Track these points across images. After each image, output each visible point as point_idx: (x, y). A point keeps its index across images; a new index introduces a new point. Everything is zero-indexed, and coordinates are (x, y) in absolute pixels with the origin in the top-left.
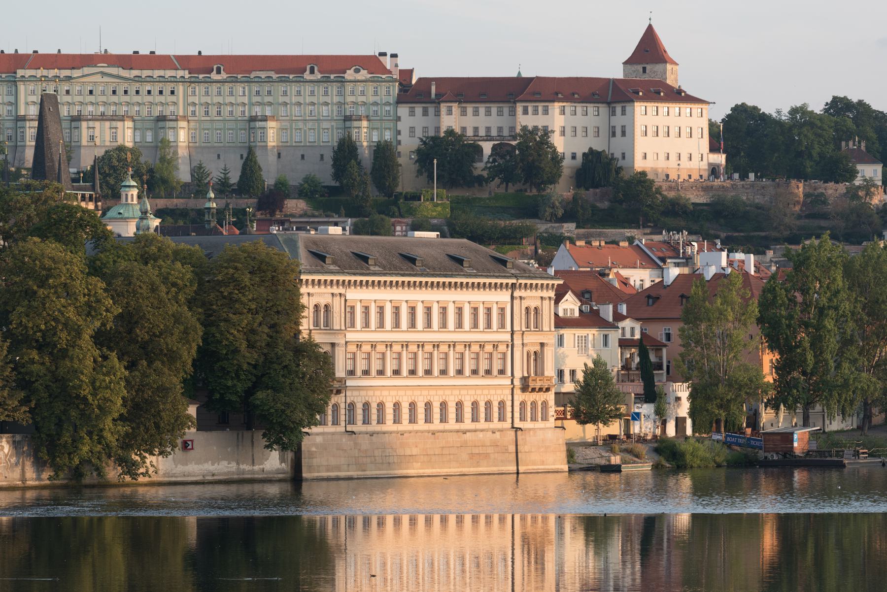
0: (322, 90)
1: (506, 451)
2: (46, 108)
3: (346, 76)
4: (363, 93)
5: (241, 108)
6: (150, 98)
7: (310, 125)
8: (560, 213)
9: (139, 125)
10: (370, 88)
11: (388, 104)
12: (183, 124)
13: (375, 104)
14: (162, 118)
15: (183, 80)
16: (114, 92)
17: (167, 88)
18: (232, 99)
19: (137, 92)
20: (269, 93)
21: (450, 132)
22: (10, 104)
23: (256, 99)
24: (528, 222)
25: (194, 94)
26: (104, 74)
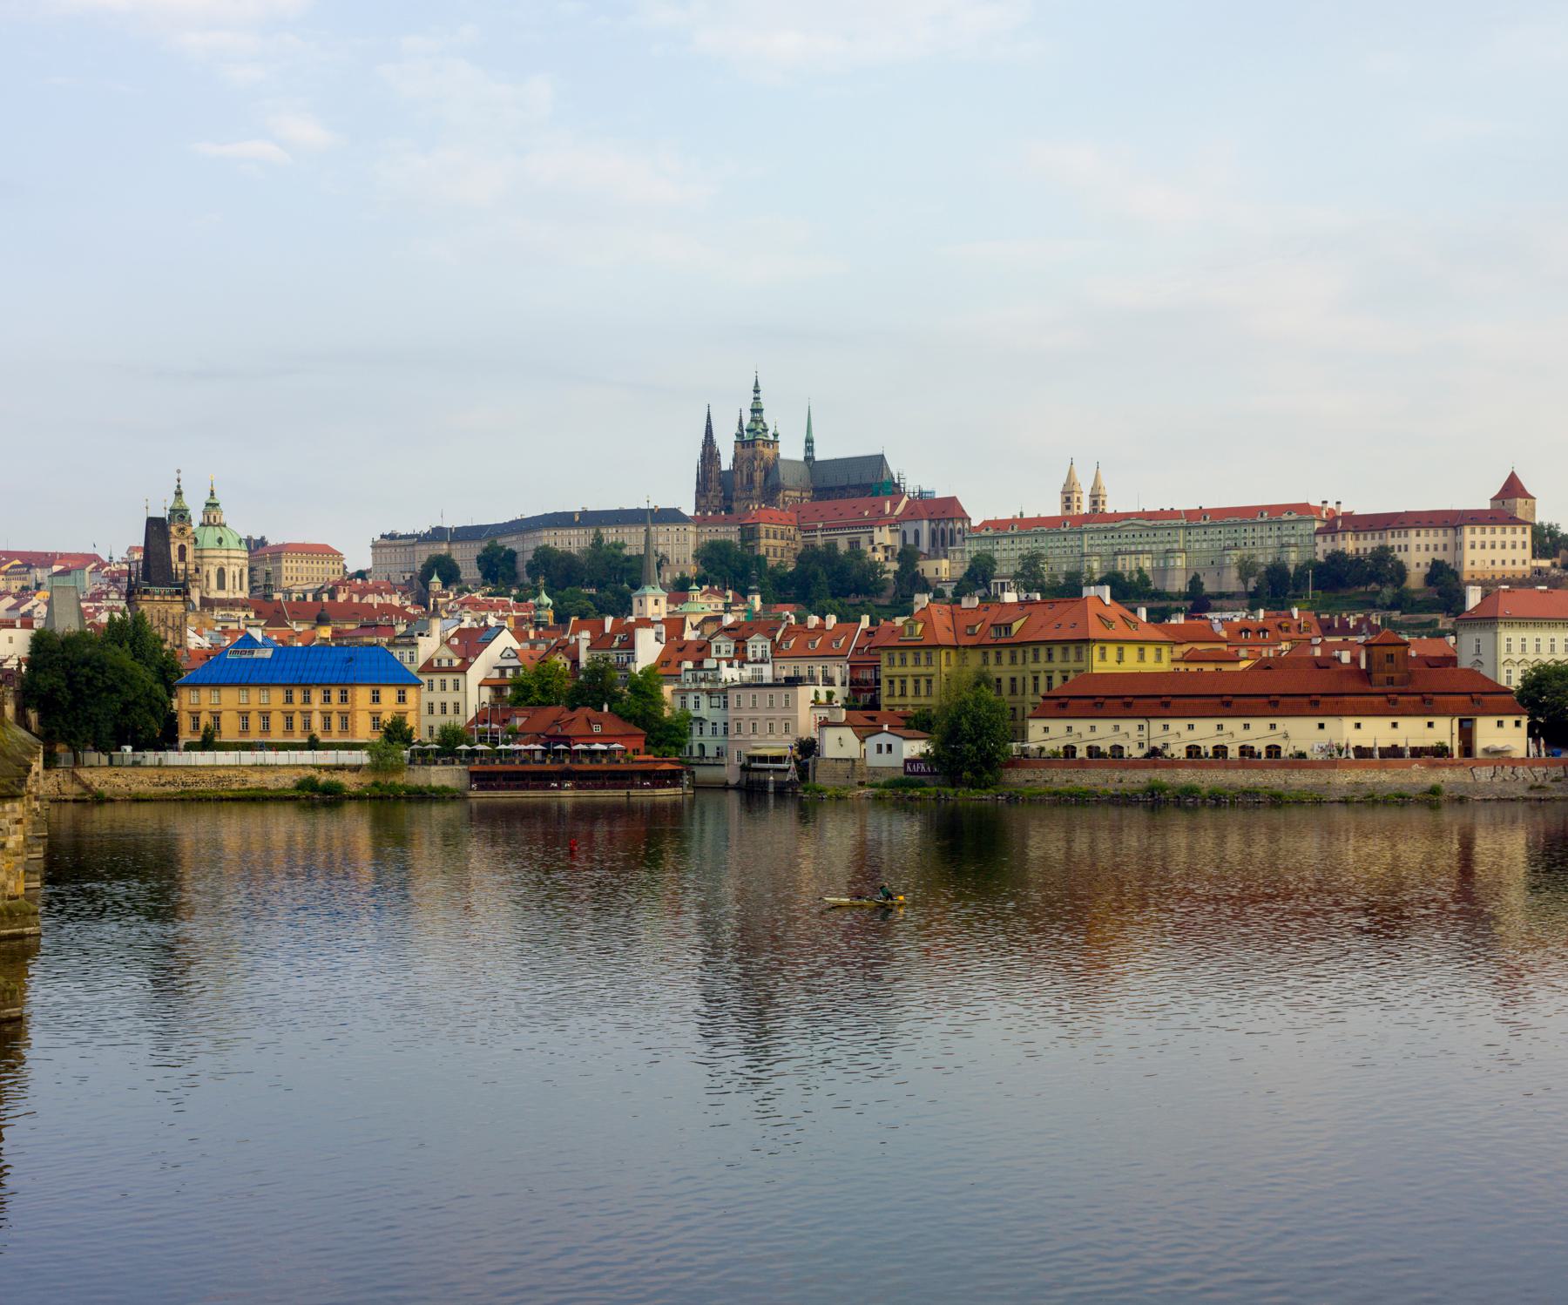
11: (1309, 535)
17: (1173, 532)
22: (1078, 546)
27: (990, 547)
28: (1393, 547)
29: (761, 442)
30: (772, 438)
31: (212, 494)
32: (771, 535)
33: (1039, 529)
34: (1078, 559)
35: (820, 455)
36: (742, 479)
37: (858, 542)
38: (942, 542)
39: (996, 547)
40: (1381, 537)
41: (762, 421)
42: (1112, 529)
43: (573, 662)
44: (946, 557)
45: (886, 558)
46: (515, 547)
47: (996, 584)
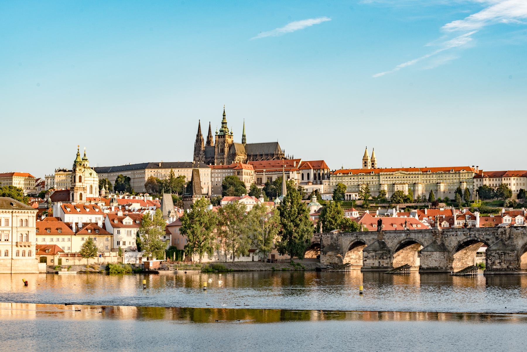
0: (455, 176)
1: (6, 266)
4: (465, 176)
5: (435, 181)
6: (412, 179)
7: (452, 184)
8: (509, 205)
10: (467, 175)
11: (471, 178)
12: (421, 185)
13: (468, 179)
14: (415, 184)
16: (404, 177)
17: (417, 176)
18: (433, 178)
19: (409, 177)
20: (442, 176)
21: (485, 185)
24: (500, 208)
25: (423, 177)
26: (401, 173)
27: (341, 181)
28: (507, 184)
30: (230, 134)
31: (85, 155)
32: (246, 174)
33: (362, 174)
34: (378, 186)
35: (248, 142)
36: (218, 150)
38: (319, 179)
40: (499, 180)
42: (393, 174)
43: (449, 224)
44: (321, 184)
46: (130, 176)
47: (347, 195)
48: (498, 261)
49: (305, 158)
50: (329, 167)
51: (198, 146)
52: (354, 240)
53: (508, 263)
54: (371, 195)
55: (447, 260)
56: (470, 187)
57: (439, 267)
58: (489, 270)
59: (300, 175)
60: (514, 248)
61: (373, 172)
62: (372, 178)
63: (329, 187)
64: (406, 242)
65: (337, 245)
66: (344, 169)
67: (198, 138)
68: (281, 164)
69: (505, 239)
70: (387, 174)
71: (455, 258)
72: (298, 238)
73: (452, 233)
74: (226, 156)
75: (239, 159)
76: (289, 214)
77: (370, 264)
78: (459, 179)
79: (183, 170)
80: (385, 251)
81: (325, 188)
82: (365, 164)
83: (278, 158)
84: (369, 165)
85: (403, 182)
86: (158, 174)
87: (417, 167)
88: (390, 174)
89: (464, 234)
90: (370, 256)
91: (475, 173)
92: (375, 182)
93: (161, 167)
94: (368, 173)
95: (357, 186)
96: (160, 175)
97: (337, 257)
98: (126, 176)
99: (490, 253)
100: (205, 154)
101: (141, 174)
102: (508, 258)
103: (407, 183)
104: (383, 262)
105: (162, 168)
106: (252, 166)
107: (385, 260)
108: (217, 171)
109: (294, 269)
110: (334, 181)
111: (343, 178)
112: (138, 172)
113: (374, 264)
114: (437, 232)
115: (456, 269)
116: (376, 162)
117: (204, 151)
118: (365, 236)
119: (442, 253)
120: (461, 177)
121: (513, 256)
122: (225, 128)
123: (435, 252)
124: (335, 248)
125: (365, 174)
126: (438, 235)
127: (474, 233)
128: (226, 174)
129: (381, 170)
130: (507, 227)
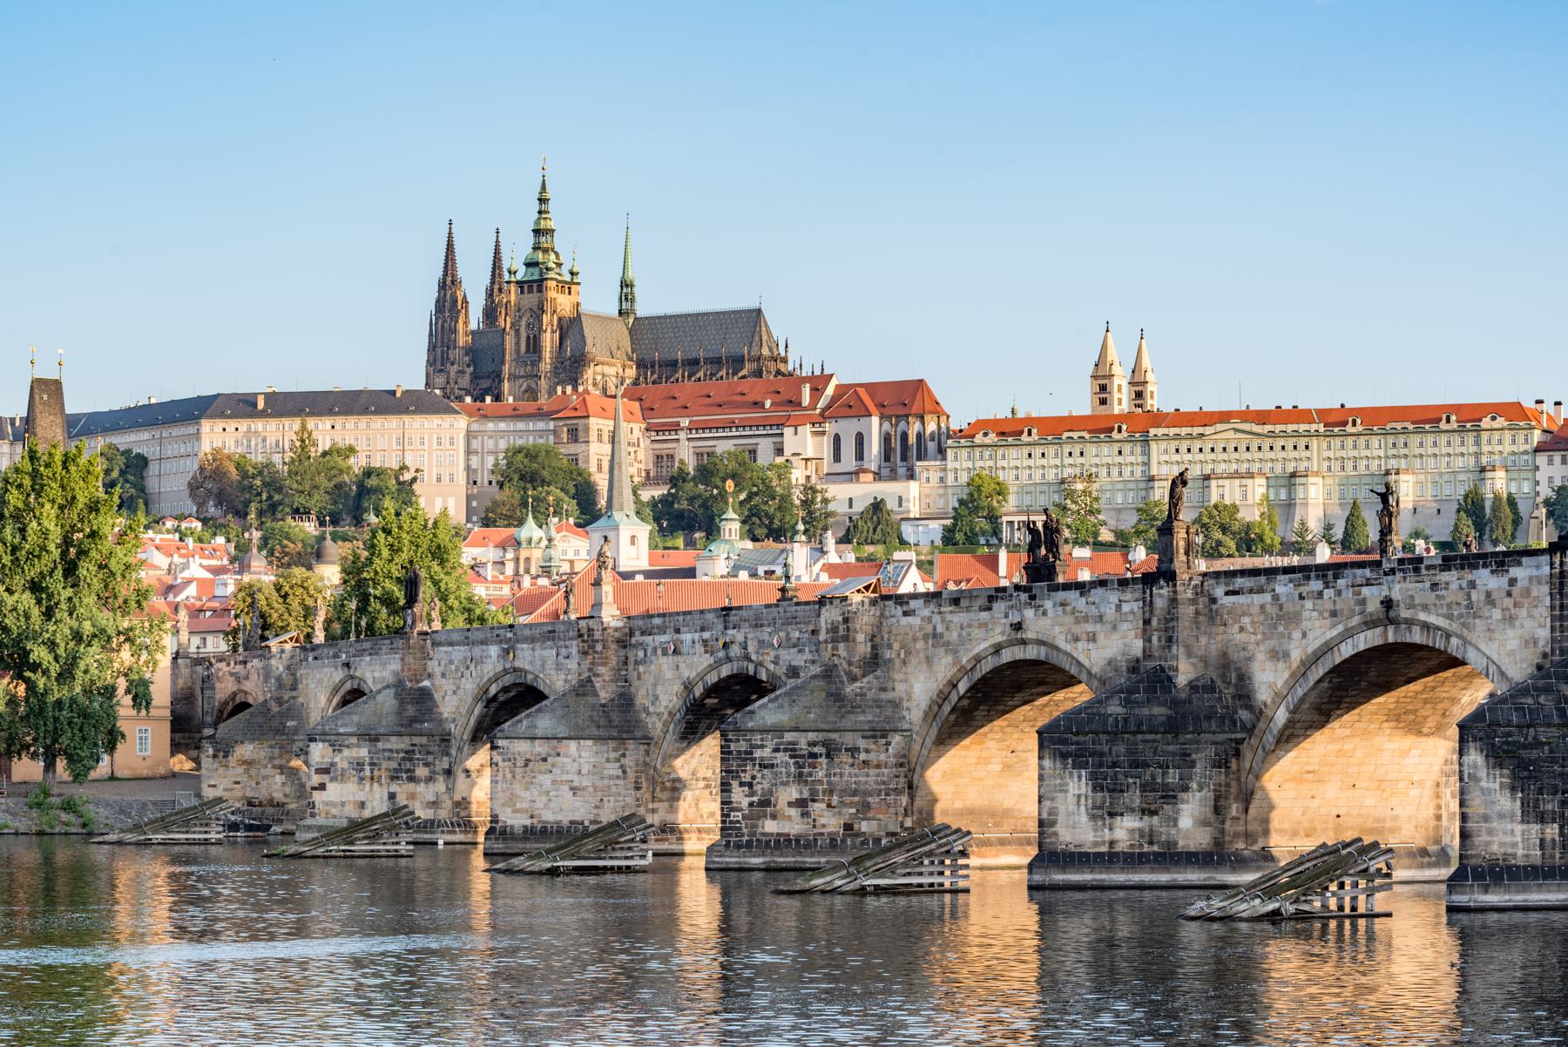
2: (37, 396)
3: (1481, 424)
5: (1377, 462)
6: (1284, 454)
7: (1446, 478)
9: (1272, 482)
10: (1507, 436)
11: (1526, 452)
13: (1514, 453)
14: (1293, 475)
15: (1317, 434)
16: (1248, 449)
17: (1302, 442)
18: (1368, 453)
19: (1271, 448)
20: (1406, 445)
23: (1392, 452)
25: (1329, 447)
26: (1236, 430)
27: (991, 463)
29: (554, 283)
30: (567, 278)
33: (1075, 435)
34: (1142, 485)
35: (644, 308)
37: (753, 452)
39: (1000, 463)
41: (553, 249)
44: (911, 476)
45: (808, 478)
47: (1011, 523)
48: (793, 793)
49: (846, 372)
50: (946, 406)
51: (443, 326)
52: (343, 683)
53: (851, 805)
54: (1104, 523)
55: (638, 789)
56: (1519, 487)
57: (591, 822)
58: (738, 846)
59: (826, 443)
60: (888, 720)
61: (1124, 427)
62: (1120, 452)
63: (941, 491)
64: (505, 690)
65: (289, 709)
66: (1020, 415)
67: (445, 295)
68: (750, 398)
69: (845, 665)
70: (1178, 437)
71: (683, 773)
72: (55, 669)
73: (663, 638)
74: (546, 364)
75: (599, 378)
76: (15, 549)
77: (343, 804)
78: (1477, 455)
79: (351, 422)
80: (424, 740)
81: (927, 496)
82: (1103, 392)
83: (758, 373)
84: (1120, 400)
85: (1243, 468)
86: (253, 443)
87: (1307, 403)
88: (1190, 436)
89: (705, 642)
90: (345, 765)
91: (1544, 431)
92: (1129, 469)
93: (263, 411)
94: (1100, 428)
95: (1056, 488)
96: (260, 446)
97: (282, 769)
98: (127, 452)
99: (743, 746)
100: (474, 362)
101: (185, 439)
102: (847, 773)
103: (1260, 473)
104: (412, 796)
105: (269, 416)
106: (637, 404)
107: (421, 788)
108: (490, 426)
109: (34, 829)
110: (960, 465)
111: (1000, 452)
112: (177, 431)
113: (362, 805)
114: (598, 635)
115: (694, 836)
116: (1150, 388)
117: (469, 351)
118: (370, 664)
119: (609, 750)
120: (1485, 449)
121: (878, 766)
122: (546, 251)
123: (573, 745)
124: (276, 723)
125: (1087, 436)
126: (599, 647)
127: (740, 638)
128: (531, 438)
129: (1158, 419)
130: (857, 598)
